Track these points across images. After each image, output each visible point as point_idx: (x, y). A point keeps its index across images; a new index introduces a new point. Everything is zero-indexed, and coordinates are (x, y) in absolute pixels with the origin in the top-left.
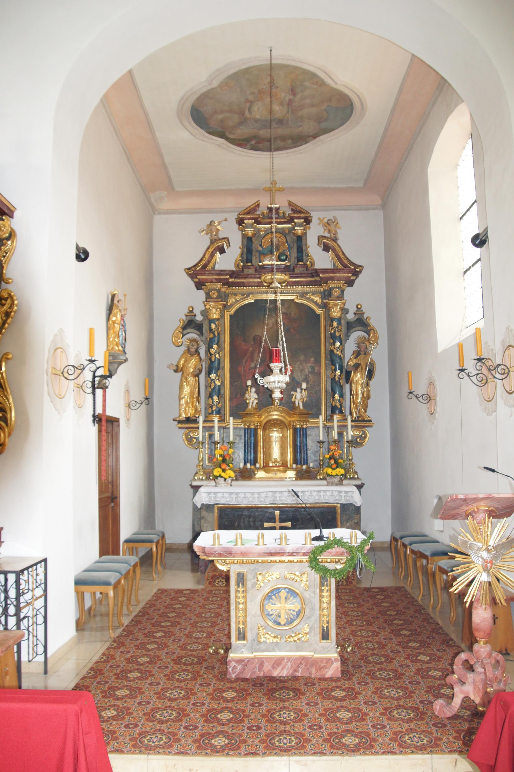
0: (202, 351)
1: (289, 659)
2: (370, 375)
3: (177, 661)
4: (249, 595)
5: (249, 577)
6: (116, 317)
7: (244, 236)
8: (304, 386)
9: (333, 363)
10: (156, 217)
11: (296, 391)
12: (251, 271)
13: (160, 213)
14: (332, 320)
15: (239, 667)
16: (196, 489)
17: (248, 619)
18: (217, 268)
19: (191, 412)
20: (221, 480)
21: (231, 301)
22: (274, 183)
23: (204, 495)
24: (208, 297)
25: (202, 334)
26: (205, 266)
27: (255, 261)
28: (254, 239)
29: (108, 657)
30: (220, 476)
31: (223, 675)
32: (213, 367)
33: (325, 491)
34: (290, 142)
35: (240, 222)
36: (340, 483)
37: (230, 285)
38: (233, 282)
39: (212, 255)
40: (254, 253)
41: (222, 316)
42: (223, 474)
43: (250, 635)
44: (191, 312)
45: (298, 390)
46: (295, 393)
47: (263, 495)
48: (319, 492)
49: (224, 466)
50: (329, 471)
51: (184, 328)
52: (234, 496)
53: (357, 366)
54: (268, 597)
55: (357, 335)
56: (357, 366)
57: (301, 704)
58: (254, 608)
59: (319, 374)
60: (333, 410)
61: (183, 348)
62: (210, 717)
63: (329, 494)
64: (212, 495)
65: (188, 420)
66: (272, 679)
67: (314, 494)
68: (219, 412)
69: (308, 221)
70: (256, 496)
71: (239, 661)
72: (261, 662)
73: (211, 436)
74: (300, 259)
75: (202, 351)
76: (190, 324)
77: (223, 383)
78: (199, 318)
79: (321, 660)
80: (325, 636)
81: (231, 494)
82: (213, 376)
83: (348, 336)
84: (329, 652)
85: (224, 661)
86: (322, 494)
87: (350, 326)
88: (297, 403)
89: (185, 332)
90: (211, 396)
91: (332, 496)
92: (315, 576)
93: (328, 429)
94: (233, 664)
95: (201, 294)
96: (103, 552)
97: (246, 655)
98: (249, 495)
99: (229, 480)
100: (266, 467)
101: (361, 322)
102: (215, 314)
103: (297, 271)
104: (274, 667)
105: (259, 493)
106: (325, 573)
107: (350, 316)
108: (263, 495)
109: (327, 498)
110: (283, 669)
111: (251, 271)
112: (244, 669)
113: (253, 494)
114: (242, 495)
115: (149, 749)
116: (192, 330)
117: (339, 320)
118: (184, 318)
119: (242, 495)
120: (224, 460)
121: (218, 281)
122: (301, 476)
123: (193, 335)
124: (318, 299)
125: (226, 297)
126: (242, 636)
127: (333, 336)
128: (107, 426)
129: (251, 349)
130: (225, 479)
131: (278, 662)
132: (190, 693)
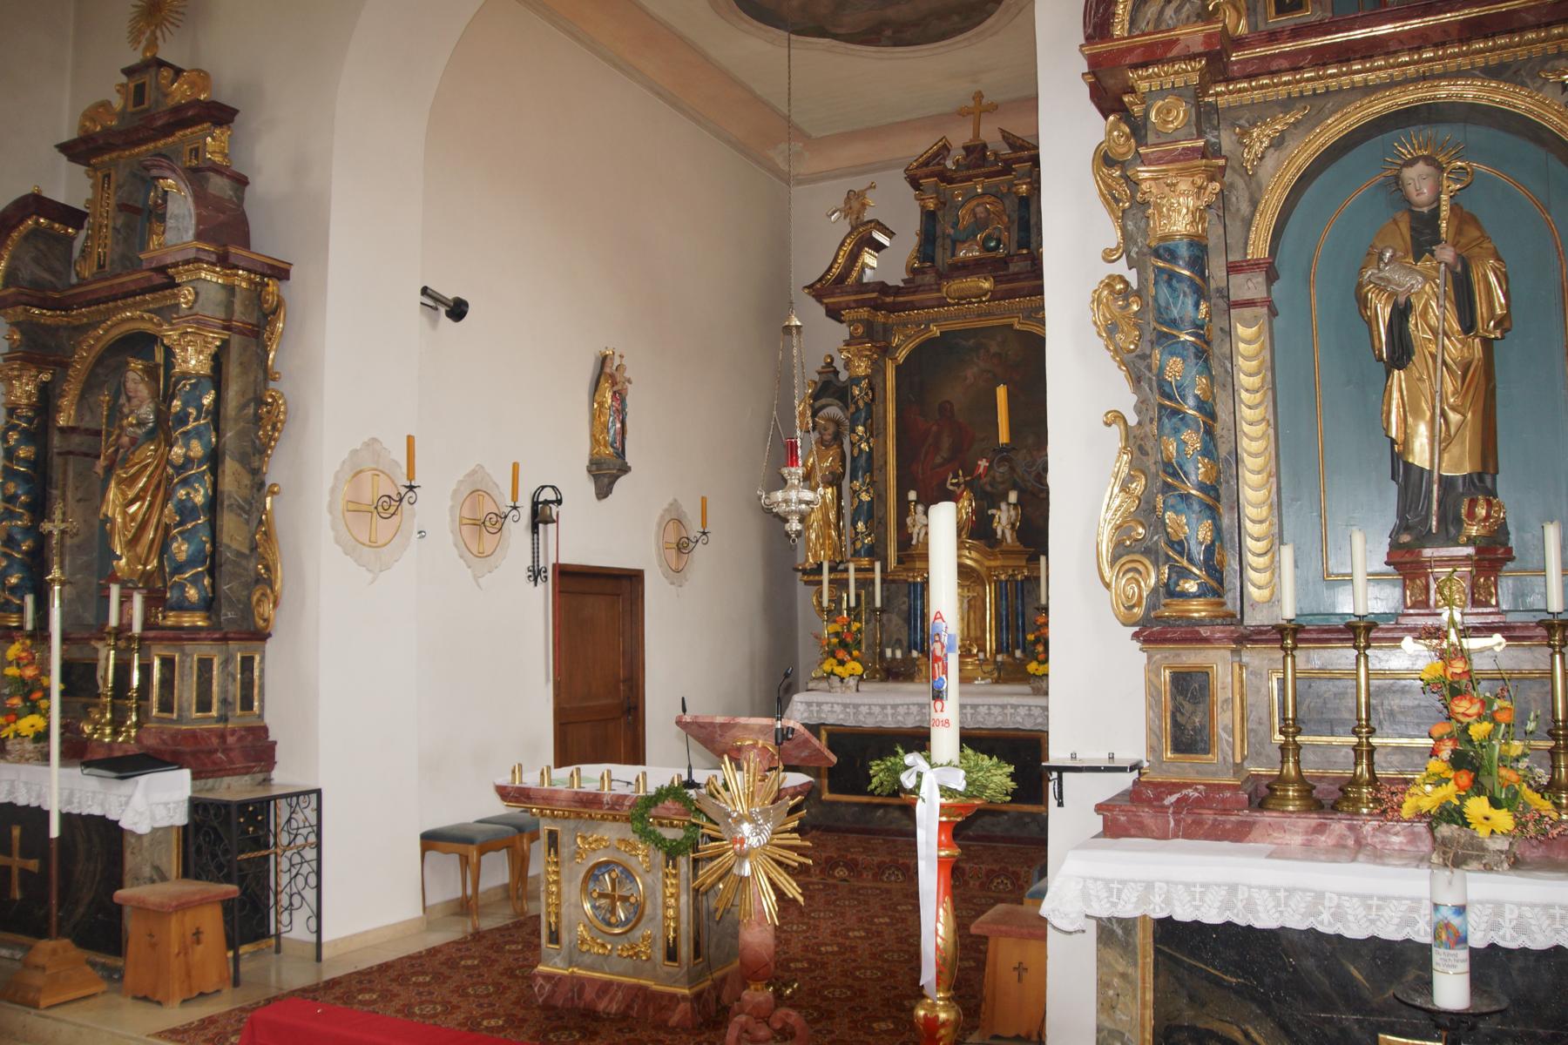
1: (620, 985)
4: (565, 871)
5: (563, 839)
8: (1013, 497)
10: (796, 191)
11: (999, 508)
12: (929, 278)
13: (800, 183)
15: (548, 987)
17: (563, 910)
20: (835, 680)
22: (979, 96)
23: (801, 707)
25: (845, 407)
26: (841, 279)
28: (940, 214)
30: (832, 673)
33: (1015, 707)
34: (956, 18)
37: (893, 308)
38: (894, 303)
39: (854, 256)
40: (939, 242)
42: (838, 670)
43: (565, 937)
44: (830, 364)
45: (1003, 506)
46: (998, 513)
47: (901, 710)
48: (1003, 707)
49: (842, 654)
52: (850, 710)
63: (1022, 711)
64: (815, 708)
67: (995, 711)
70: (889, 711)
71: (548, 977)
72: (581, 983)
76: (829, 387)
79: (662, 995)
81: (845, 706)
82: (857, 484)
86: (1009, 711)
88: (999, 532)
89: (818, 404)
91: (1030, 715)
94: (540, 981)
98: (876, 710)
99: (852, 682)
104: (599, 997)
105: (894, 707)
108: (901, 710)
109: (1019, 719)
110: (611, 1001)
111: (929, 278)
112: (553, 992)
113: (883, 707)
114: (864, 710)
116: (829, 400)
118: (816, 378)
119: (864, 710)
121: (861, 304)
125: (887, 330)
126: (555, 937)
129: (935, 428)
130: (842, 680)
131: (605, 988)
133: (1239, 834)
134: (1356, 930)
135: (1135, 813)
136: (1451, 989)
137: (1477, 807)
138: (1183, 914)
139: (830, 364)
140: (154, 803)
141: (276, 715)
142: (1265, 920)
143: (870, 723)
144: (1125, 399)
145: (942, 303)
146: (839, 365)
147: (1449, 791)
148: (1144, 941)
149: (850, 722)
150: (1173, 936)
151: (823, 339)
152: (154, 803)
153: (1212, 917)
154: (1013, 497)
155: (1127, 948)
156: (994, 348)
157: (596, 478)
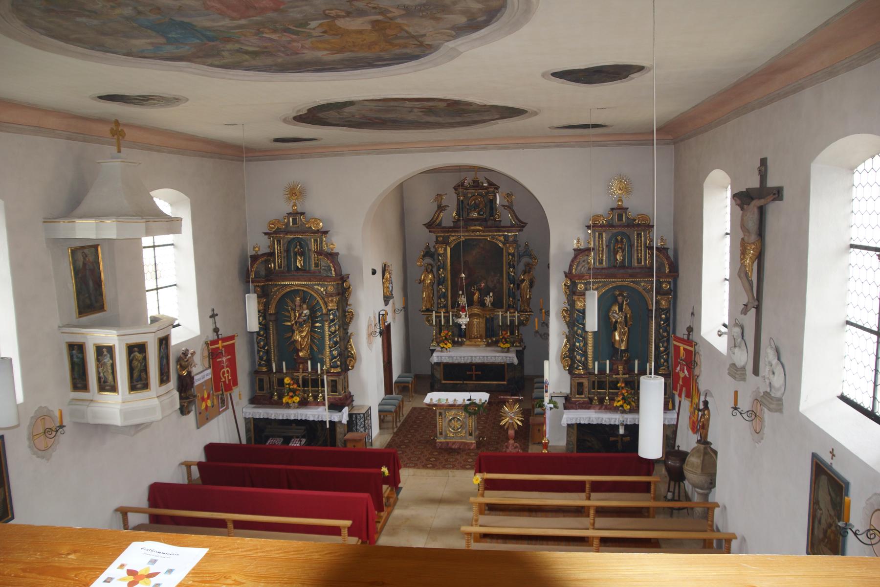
0: (435, 270)
2: (531, 285)
3: (419, 442)
6: (387, 275)
7: (458, 199)
8: (491, 294)
9: (509, 279)
14: (509, 254)
16: (433, 351)
18: (443, 225)
19: (429, 306)
21: (452, 238)
24: (437, 242)
25: (434, 260)
27: (465, 215)
29: (393, 440)
31: (435, 447)
32: (441, 282)
35: (455, 188)
36: (508, 350)
41: (445, 250)
44: (428, 246)
50: (502, 345)
51: (424, 256)
53: (523, 280)
54: (450, 420)
55: (525, 260)
56: (523, 280)
57: (458, 457)
58: (445, 424)
59: (502, 283)
60: (509, 307)
61: (423, 268)
62: (428, 460)
65: (428, 310)
66: (451, 449)
68: (445, 306)
69: (497, 188)
72: (448, 443)
73: (440, 321)
74: (492, 215)
75: (435, 270)
76: (428, 253)
77: (446, 290)
78: (433, 250)
80: (471, 434)
83: (519, 261)
84: (472, 440)
85: (435, 443)
87: (520, 257)
90: (439, 298)
92: (467, 415)
93: (504, 318)
95: (433, 236)
96: (386, 393)
97: (442, 440)
100: (470, 338)
101: (527, 253)
102: (441, 251)
103: (490, 223)
106: (470, 414)
107: (522, 249)
115: (409, 467)
117: (513, 255)
120: (446, 339)
122: (488, 345)
123: (428, 260)
124: (502, 238)
126: (441, 434)
127: (509, 264)
128: (386, 333)
131: (454, 443)
132: (422, 452)
133: (589, 408)
134: (607, 423)
135: (569, 403)
136: (622, 431)
137: (625, 405)
138: (582, 422)
139: (428, 246)
140: (343, 416)
141: (352, 389)
142: (595, 422)
143: (456, 362)
144: (567, 330)
145: (468, 231)
146: (431, 246)
147: (621, 403)
148: (575, 427)
149: (451, 361)
150: (580, 426)
151: (429, 238)
152: (343, 416)
153: (587, 422)
154: (491, 294)
155: (573, 428)
156: (482, 245)
157: (385, 301)
